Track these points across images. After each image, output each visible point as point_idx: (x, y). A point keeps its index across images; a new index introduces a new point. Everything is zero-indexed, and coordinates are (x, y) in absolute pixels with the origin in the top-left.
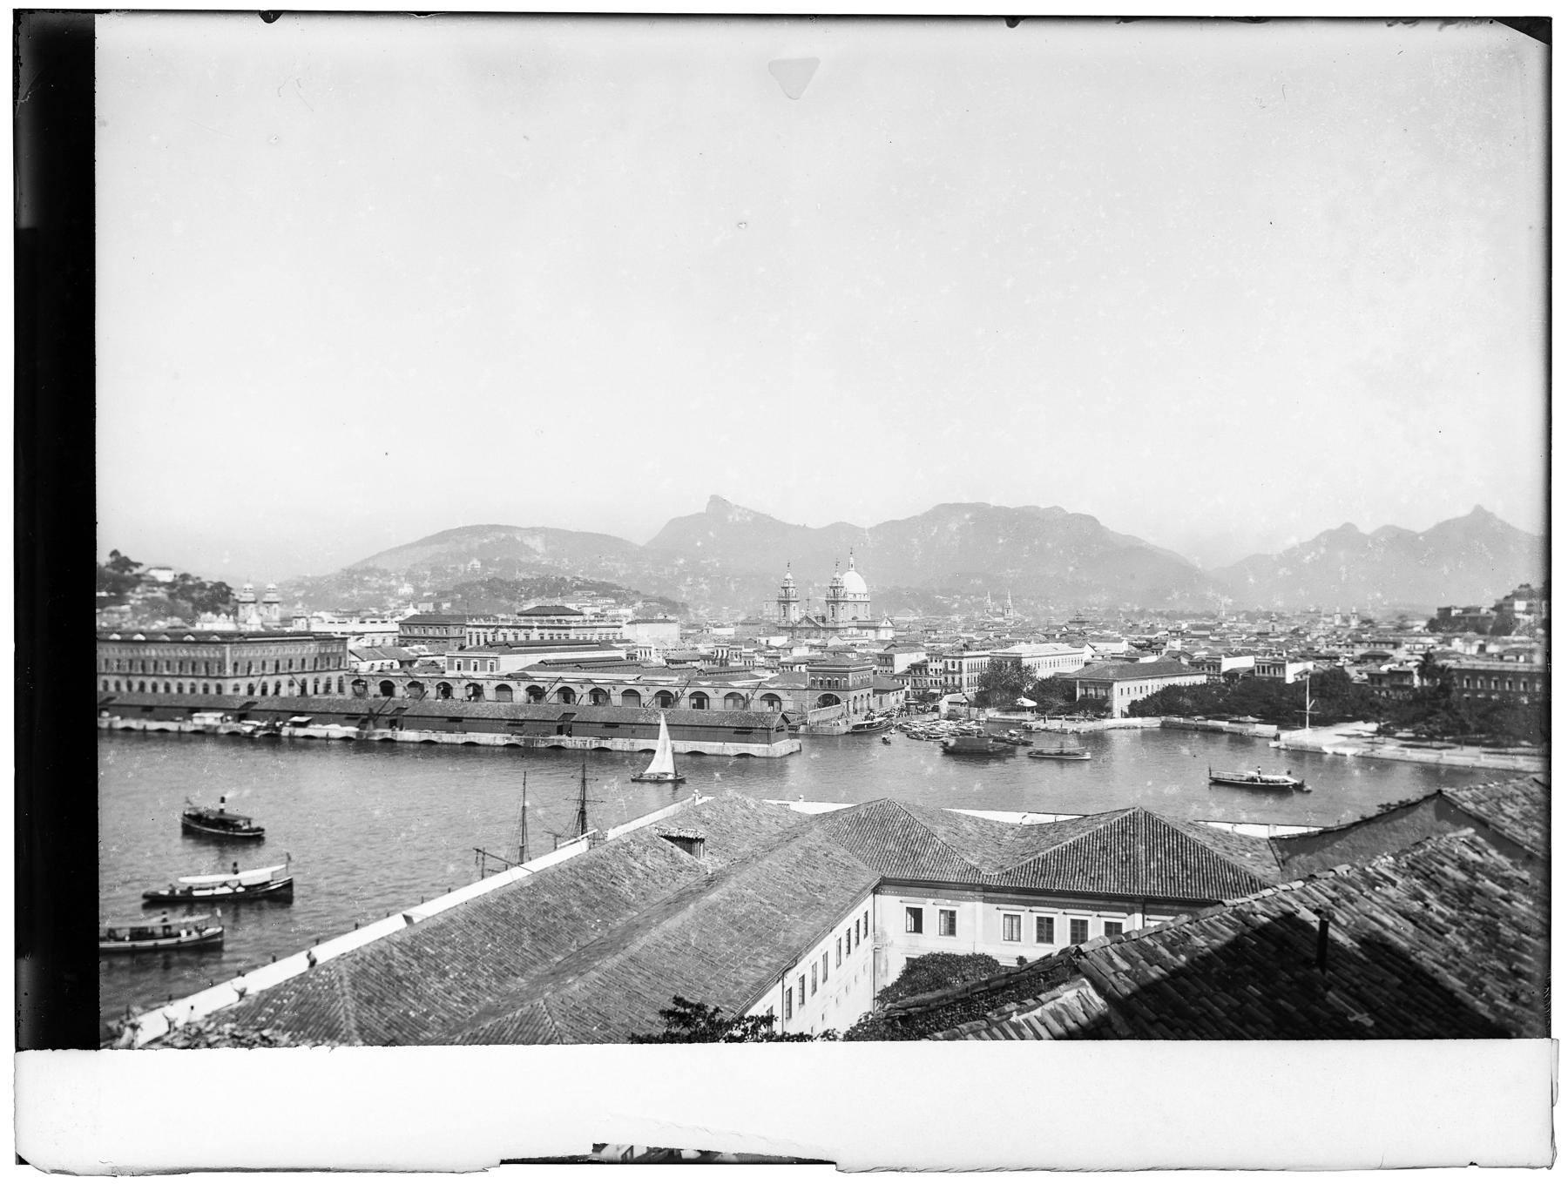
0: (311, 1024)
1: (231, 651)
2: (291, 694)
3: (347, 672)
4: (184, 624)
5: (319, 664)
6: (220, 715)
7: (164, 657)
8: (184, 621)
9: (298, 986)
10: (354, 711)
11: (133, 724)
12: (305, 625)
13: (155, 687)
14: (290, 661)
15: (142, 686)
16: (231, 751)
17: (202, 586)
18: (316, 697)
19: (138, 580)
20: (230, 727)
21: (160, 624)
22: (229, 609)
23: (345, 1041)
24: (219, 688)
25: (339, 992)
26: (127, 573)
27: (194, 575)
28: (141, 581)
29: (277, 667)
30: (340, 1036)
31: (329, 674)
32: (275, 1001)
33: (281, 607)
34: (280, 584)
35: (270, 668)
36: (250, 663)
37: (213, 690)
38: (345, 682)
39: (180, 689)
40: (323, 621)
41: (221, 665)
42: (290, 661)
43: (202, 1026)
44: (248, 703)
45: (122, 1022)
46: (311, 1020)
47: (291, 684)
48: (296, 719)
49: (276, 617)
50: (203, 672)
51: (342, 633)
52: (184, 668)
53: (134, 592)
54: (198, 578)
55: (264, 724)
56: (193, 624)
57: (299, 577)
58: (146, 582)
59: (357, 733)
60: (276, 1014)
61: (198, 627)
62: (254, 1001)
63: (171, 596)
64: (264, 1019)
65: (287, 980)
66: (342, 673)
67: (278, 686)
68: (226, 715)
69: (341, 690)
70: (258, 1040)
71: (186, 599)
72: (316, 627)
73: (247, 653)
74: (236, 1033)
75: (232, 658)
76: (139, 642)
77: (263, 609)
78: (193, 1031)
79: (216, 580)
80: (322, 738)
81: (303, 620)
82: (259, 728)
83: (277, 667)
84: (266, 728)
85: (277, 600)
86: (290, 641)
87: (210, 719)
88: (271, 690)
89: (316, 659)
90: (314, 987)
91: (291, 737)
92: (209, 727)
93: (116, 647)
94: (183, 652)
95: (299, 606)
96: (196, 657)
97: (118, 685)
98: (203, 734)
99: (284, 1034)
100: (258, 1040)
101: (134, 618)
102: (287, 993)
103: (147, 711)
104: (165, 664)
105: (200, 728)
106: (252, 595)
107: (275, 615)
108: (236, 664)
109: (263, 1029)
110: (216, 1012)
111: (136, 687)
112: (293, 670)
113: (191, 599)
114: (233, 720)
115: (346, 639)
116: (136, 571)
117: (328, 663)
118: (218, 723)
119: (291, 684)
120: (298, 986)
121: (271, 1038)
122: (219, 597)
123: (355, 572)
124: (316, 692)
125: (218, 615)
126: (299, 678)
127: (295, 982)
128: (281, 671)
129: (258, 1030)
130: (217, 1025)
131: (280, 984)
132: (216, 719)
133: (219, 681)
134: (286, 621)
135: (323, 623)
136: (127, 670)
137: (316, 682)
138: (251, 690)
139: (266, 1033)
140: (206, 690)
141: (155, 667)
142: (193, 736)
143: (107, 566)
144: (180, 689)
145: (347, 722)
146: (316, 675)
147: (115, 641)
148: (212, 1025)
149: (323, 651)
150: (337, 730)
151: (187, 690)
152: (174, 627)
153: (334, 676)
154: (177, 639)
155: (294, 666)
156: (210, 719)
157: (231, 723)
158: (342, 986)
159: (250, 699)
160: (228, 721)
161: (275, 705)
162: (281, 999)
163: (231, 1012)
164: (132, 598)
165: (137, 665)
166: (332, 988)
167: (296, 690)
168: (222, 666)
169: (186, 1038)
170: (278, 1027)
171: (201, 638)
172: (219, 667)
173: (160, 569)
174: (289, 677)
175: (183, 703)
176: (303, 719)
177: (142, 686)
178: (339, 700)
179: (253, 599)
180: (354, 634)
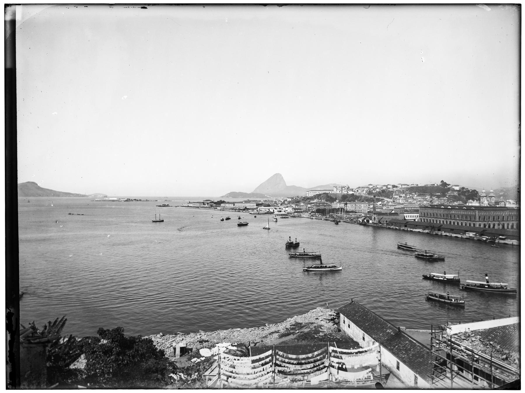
0: (508, 344)
1: (478, 212)
2: (499, 228)
4: (463, 204)
5: (509, 218)
6: (474, 233)
7: (457, 214)
8: (463, 202)
11: (448, 234)
12: (504, 204)
13: (454, 223)
14: (499, 217)
15: (450, 222)
17: (468, 191)
18: (508, 230)
19: (449, 189)
20: (478, 238)
21: (456, 203)
22: (477, 199)
24: (474, 224)
26: (446, 187)
27: (466, 188)
29: (494, 218)
31: (513, 222)
32: (494, 333)
33: (495, 198)
34: (495, 190)
35: (491, 219)
36: (484, 217)
37: (472, 225)
39: (462, 224)
40: (510, 203)
43: (470, 334)
44: (484, 230)
45: (445, 326)
47: (499, 225)
48: (501, 237)
49: (493, 202)
50: (469, 219)
52: (463, 218)
53: (448, 193)
54: (467, 189)
55: (489, 238)
56: (466, 203)
57: (501, 188)
58: (451, 190)
61: (467, 204)
62: (487, 331)
63: (459, 194)
64: (491, 338)
67: (494, 225)
68: (477, 234)
70: (489, 344)
71: (464, 195)
72: (508, 205)
73: (483, 213)
74: (481, 340)
75: (478, 215)
76: (450, 209)
77: (489, 199)
78: (467, 335)
79: (473, 189)
81: (503, 203)
82: (487, 239)
83: (494, 218)
84: (490, 239)
85: (494, 196)
87: (471, 234)
88: (492, 226)
89: (508, 217)
90: (508, 332)
91: (499, 243)
92: (471, 237)
93: (443, 210)
94: (462, 212)
95: (502, 198)
96: (467, 214)
97: (443, 222)
98: (470, 239)
99: (498, 345)
100: (489, 344)
101: (448, 201)
102: (499, 331)
103: (452, 230)
104: (457, 216)
105: (468, 237)
106: (485, 194)
107: (493, 200)
108: (480, 217)
109: (491, 341)
110: (475, 331)
111: (448, 223)
112: (500, 220)
113: (465, 195)
114: (479, 235)
116: (448, 187)
117: (513, 218)
118: (474, 236)
119: (499, 225)
121: (493, 345)
122: (474, 195)
124: (508, 228)
125: (474, 201)
126: (502, 223)
127: (501, 328)
128: (495, 220)
129: (488, 341)
130: (475, 335)
131: (496, 328)
132: (473, 234)
133: (474, 222)
134: (497, 203)
137: (508, 224)
138: (485, 226)
139: (491, 343)
140: (470, 225)
141: (454, 216)
142: (466, 239)
144: (462, 224)
146: (508, 222)
148: (473, 335)
149: (511, 214)
151: (464, 225)
152: (460, 204)
154: (460, 208)
155: (500, 219)
156: (471, 234)
157: (478, 236)
160: (477, 235)
161: (493, 232)
162: (497, 332)
163: (479, 332)
164: (447, 195)
167: (501, 227)
168: (475, 218)
169: (465, 337)
170: (496, 342)
172: (474, 218)
173: (456, 186)
175: (463, 229)
176: (504, 237)
177: (450, 222)
179: (485, 195)
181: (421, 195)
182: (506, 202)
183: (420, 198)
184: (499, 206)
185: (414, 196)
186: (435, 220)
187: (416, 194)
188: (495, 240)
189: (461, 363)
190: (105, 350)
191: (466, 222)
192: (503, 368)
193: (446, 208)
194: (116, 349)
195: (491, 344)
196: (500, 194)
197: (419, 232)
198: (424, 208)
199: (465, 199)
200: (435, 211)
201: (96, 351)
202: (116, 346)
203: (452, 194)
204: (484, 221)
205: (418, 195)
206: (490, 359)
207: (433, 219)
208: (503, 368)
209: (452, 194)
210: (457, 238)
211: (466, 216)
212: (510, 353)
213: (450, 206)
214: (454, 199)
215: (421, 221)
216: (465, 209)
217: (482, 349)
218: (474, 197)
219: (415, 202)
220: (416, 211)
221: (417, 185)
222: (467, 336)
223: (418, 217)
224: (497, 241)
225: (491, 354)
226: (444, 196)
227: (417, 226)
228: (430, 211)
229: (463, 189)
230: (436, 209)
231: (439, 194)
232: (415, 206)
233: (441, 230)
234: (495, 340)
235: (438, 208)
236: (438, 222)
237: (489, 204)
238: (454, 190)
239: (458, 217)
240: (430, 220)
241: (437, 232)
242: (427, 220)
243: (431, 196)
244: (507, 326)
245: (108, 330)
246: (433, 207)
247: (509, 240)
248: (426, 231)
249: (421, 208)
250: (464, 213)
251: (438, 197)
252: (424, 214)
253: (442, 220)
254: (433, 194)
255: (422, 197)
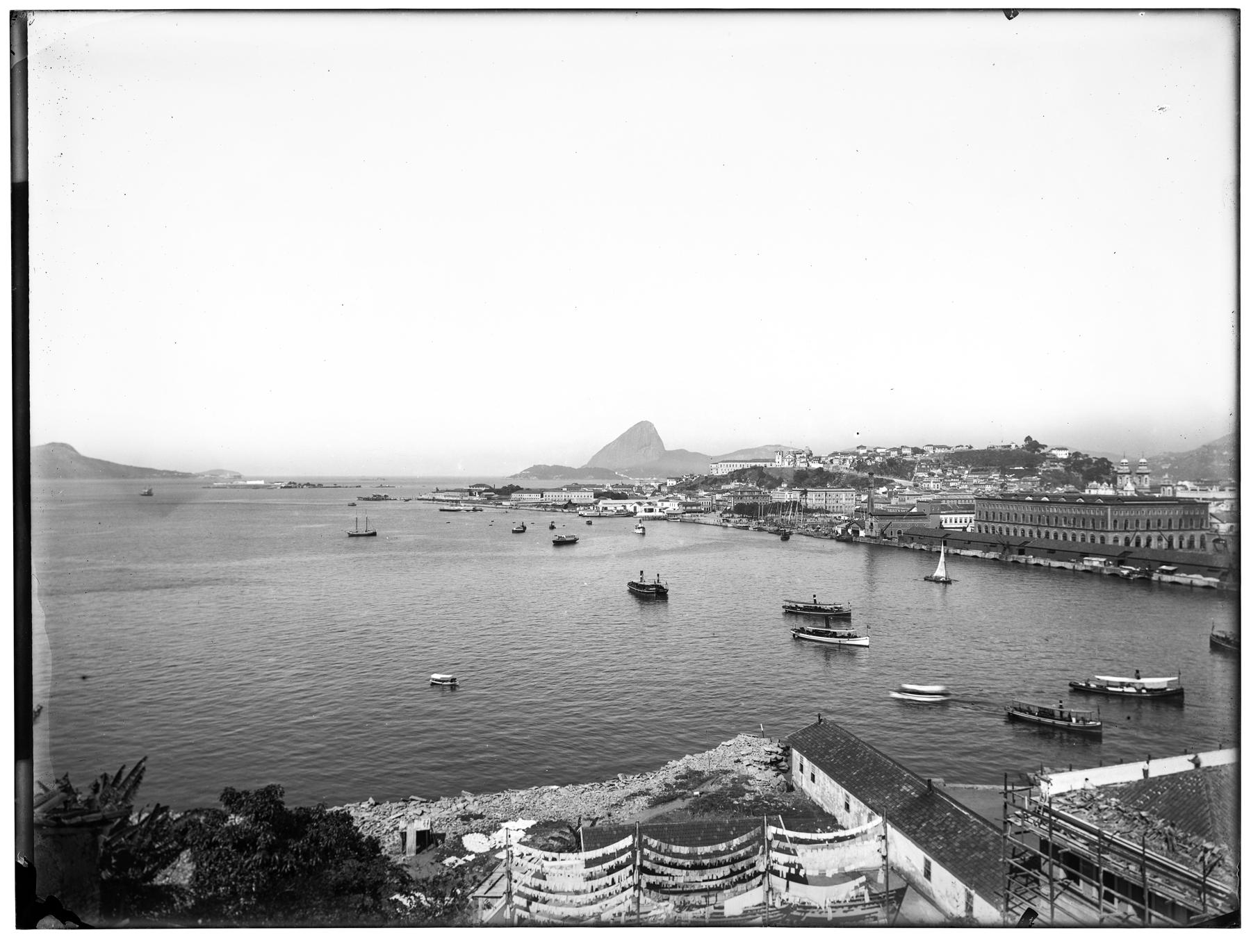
0: (1182, 817)
2: (1160, 547)
3: (1208, 532)
4: (1077, 490)
5: (1183, 524)
6: (1103, 560)
9: (1170, 784)
10: (1214, 565)
11: (1042, 562)
13: (1056, 536)
14: (1159, 520)
15: (1047, 534)
16: (1110, 587)
17: (1089, 461)
18: (1181, 551)
23: (1212, 841)
24: (1103, 539)
25: (1205, 798)
26: (1036, 453)
27: (1083, 453)
28: (1045, 459)
29: (1148, 525)
30: (1207, 835)
31: (1193, 533)
34: (1150, 459)
36: (1126, 521)
37: (1098, 541)
38: (1206, 540)
39: (1074, 538)
40: (1186, 489)
41: (1104, 520)
42: (1159, 520)
43: (1094, 794)
44: (1125, 552)
46: (1182, 814)
47: (1160, 539)
48: (1164, 567)
49: (1147, 486)
50: (1091, 528)
51: (1203, 499)
52: (1076, 523)
54: (1087, 455)
56: (1083, 489)
57: (1165, 453)
59: (1218, 583)
60: (1152, 802)
61: (1087, 492)
62: (1134, 786)
63: (1066, 469)
65: (1161, 777)
66: (1204, 532)
67: (1149, 540)
69: (1203, 544)
72: (1181, 494)
73: (1123, 513)
74: (1120, 807)
75: (1112, 516)
77: (1136, 479)
78: (1088, 796)
79: (1099, 457)
80: (1186, 585)
81: (1170, 488)
82: (1134, 572)
83: (1148, 525)
85: (1147, 471)
86: (1159, 504)
87: (1096, 562)
88: (1143, 542)
89: (1181, 520)
90: (1183, 788)
91: (1160, 581)
92: (1095, 568)
93: (1030, 506)
94: (1074, 511)
95: (1166, 476)
97: (1031, 533)
98: (1092, 573)
101: (1041, 484)
102: (1161, 787)
103: (1051, 553)
105: (1089, 569)
107: (1146, 483)
108: (1115, 521)
109: (1142, 810)
111: (1043, 535)
112: (1161, 528)
113: (1081, 471)
115: (1208, 504)
116: (1042, 451)
117: (1192, 524)
119: (1160, 539)
120: (1170, 784)
122: (1101, 469)
123: (1215, 447)
124: (1181, 547)
126: (1167, 534)
127: (1167, 779)
128: (1151, 528)
129: (1137, 809)
130: (1105, 797)
132: (1100, 562)
133: (1102, 534)
134: (1155, 488)
135: (1186, 490)
136: (1037, 523)
137: (1181, 539)
138: (1127, 542)
139: (1144, 814)
140: (1093, 540)
141: (1056, 521)
143: (1023, 448)
144: (1074, 538)
145: (1209, 573)
146: (1181, 533)
147: (1029, 501)
148: (1102, 795)
149: (1187, 513)
150: (1199, 580)
151: (1079, 539)
152: (1070, 492)
153: (1197, 535)
154: (1071, 500)
156: (1096, 562)
157: (1112, 567)
158: (1208, 795)
159: (1126, 549)
160: (1109, 565)
161: (1147, 555)
162: (1156, 790)
163: (1116, 789)
165: (1044, 520)
166: (1200, 793)
167: (1164, 544)
169: (1082, 800)
170: (1153, 812)
171: (1090, 501)
172: (1103, 523)
174: (1157, 534)
175: (1076, 549)
176: (1171, 568)
177: (1047, 534)
178: (1201, 555)
179: (1128, 471)
180: (1214, 499)
181: (978, 470)
182: (1177, 486)
183: (976, 479)
184: (1161, 495)
185: (963, 473)
186: (1012, 528)
187: (967, 468)
188: (1152, 576)
189: (1073, 862)
190: (239, 839)
191: (1083, 532)
192: (1170, 873)
193: (1037, 502)
194: (265, 836)
195: (1142, 818)
196: (1163, 467)
197: (975, 557)
198: (986, 502)
199: (1081, 480)
200: (1013, 508)
201: (217, 843)
202: (267, 830)
203: (1052, 468)
204: (1126, 531)
205: (973, 472)
206: (1142, 852)
207: (1007, 525)
208: (1170, 873)
209: (1052, 468)
210: (1177, 586)
211: (1084, 519)
212: (1187, 836)
213: (1047, 496)
214: (1055, 480)
215: (980, 531)
216: (1082, 503)
217: (1123, 829)
218: (1102, 476)
219: (966, 487)
220: (968, 509)
221: (971, 447)
222: (1088, 800)
223: (973, 522)
224: (1155, 577)
225: (1144, 840)
226: (1031, 471)
227: (969, 542)
228: (1000, 508)
229: (1076, 457)
230: (1014, 504)
231: (1021, 468)
232: (965, 497)
233: (1026, 551)
234: (1153, 807)
235: (1018, 501)
236: (1019, 534)
237: (1136, 491)
238: (1056, 460)
239: (1065, 521)
240: (1000, 529)
241: (1016, 557)
242: (993, 528)
243: (1004, 471)
244: (1181, 773)
245: (246, 793)
246: (1006, 499)
247: (1185, 575)
248: (992, 555)
249: (980, 501)
250: (1078, 513)
251: (1019, 475)
252: (987, 515)
253: (1027, 529)
254: (1006, 467)
255: (983, 476)
